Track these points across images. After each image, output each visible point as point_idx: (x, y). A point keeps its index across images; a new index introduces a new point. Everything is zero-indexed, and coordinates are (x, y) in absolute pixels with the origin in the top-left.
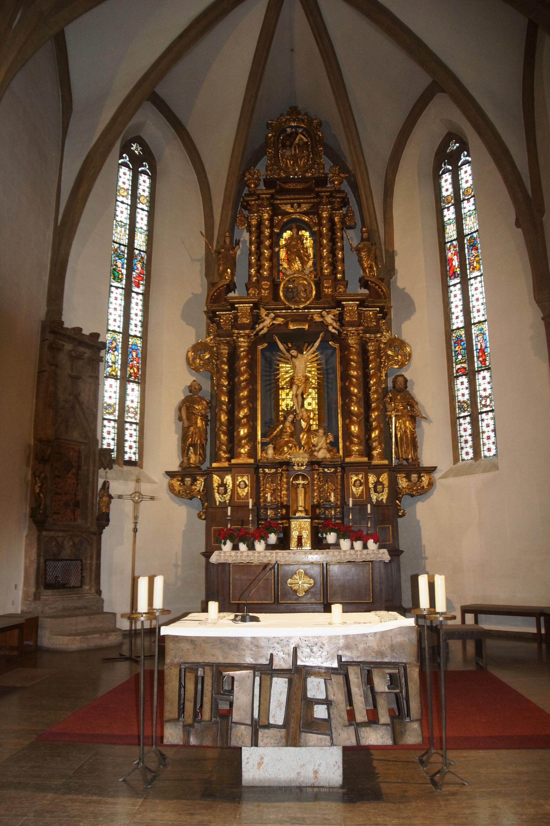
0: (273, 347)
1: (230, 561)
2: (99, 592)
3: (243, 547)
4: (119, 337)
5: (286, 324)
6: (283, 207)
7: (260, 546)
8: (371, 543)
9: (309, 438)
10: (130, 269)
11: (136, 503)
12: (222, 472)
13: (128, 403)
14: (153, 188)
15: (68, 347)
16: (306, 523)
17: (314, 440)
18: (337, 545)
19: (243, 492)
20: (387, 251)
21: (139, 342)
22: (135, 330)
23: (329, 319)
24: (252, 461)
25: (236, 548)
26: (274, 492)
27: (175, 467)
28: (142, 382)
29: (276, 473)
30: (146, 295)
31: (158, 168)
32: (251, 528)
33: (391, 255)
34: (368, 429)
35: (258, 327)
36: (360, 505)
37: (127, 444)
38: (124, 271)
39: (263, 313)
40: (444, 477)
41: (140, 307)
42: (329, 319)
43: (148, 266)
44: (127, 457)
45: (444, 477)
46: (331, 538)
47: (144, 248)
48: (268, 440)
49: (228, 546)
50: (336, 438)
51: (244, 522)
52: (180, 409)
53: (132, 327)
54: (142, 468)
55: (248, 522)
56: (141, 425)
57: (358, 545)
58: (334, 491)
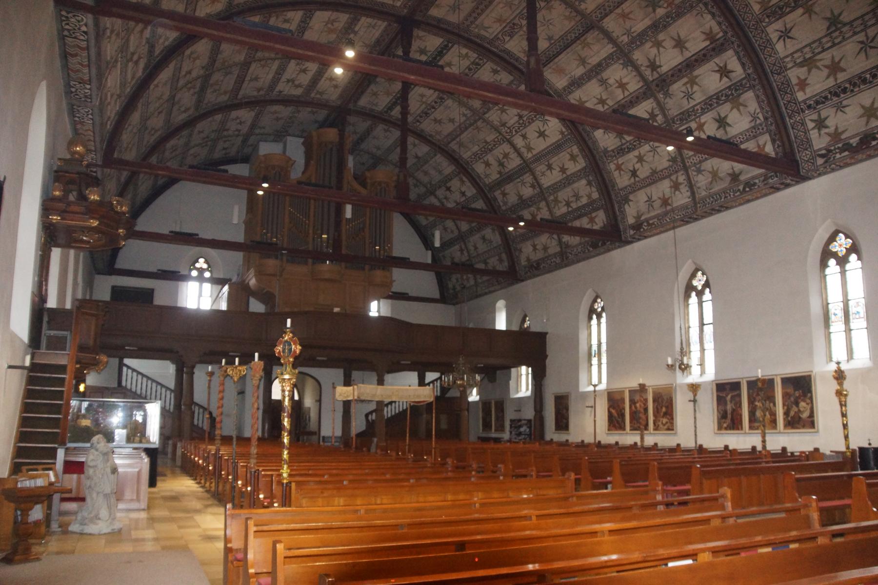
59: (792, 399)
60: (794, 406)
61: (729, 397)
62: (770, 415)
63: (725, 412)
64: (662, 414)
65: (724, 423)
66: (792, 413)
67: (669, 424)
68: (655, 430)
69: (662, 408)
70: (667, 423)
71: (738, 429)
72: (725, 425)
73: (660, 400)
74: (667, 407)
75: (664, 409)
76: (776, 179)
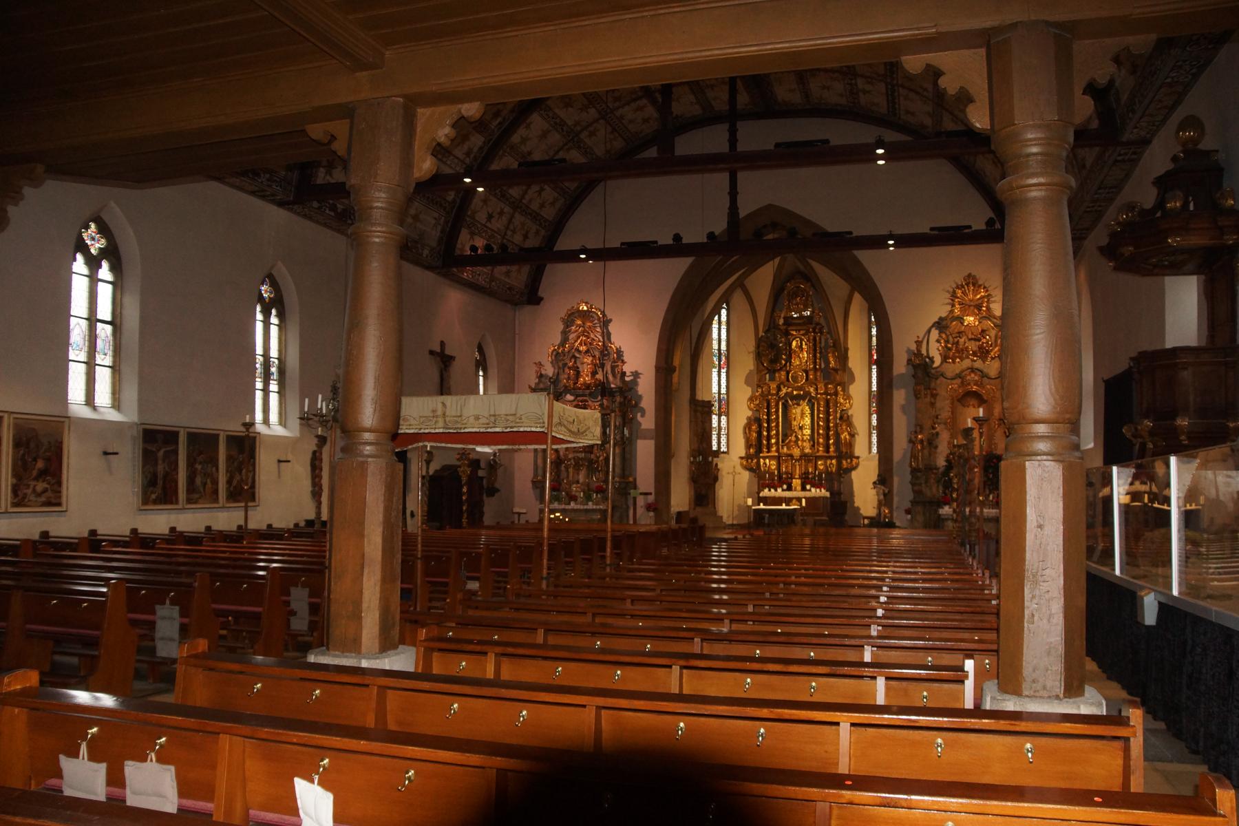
0: (787, 401)
1: (767, 496)
2: (715, 508)
3: (772, 490)
4: (717, 395)
5: (793, 392)
6: (792, 332)
7: (779, 490)
8: (823, 490)
9: (802, 443)
10: (720, 360)
11: (734, 476)
12: (764, 458)
13: (722, 425)
14: (728, 315)
15: (700, 409)
16: (799, 481)
17: (805, 444)
18: (810, 490)
19: (773, 467)
20: (844, 348)
21: (725, 396)
22: (723, 391)
23: (812, 390)
24: (777, 454)
25: (770, 490)
26: (786, 467)
27: (743, 454)
28: (727, 415)
29: (787, 459)
30: (727, 373)
31: (731, 305)
32: (776, 482)
33: (847, 350)
34: (827, 438)
35: (781, 393)
36: (820, 474)
37: (722, 444)
38: (717, 363)
39: (782, 387)
40: (863, 460)
41: (725, 379)
42: (812, 390)
43: (728, 358)
44: (722, 450)
45: (863, 460)
46: (808, 487)
47: (725, 349)
48: (783, 444)
49: (766, 490)
50: (814, 442)
51: (773, 480)
52: (745, 428)
53: (722, 389)
54: (728, 454)
55: (775, 480)
56: (728, 435)
57: (818, 490)
58: (812, 467)
59: (236, 464)
60: (237, 473)
61: (161, 454)
62: (212, 484)
63: (155, 475)
64: (35, 473)
65: (152, 493)
66: (235, 483)
67: (49, 494)
68: (15, 505)
69: (35, 460)
70: (45, 491)
71: (171, 503)
72: (153, 496)
73: (32, 445)
74: (48, 460)
75: (40, 464)
76: (278, 188)
